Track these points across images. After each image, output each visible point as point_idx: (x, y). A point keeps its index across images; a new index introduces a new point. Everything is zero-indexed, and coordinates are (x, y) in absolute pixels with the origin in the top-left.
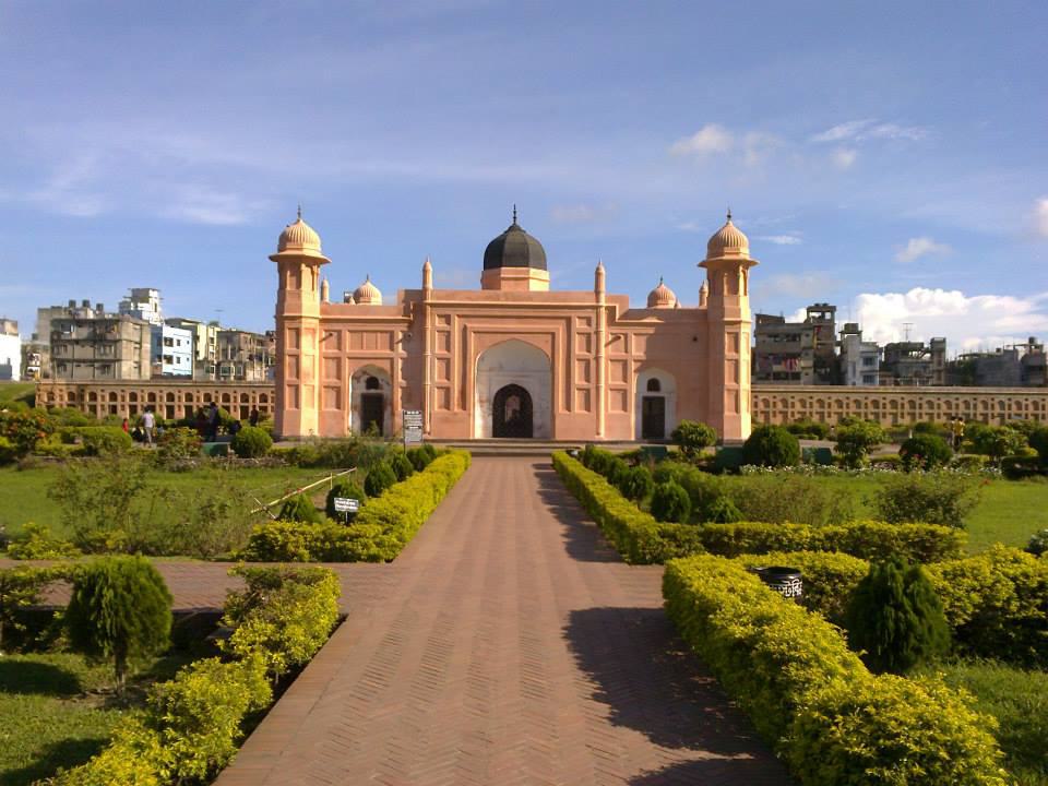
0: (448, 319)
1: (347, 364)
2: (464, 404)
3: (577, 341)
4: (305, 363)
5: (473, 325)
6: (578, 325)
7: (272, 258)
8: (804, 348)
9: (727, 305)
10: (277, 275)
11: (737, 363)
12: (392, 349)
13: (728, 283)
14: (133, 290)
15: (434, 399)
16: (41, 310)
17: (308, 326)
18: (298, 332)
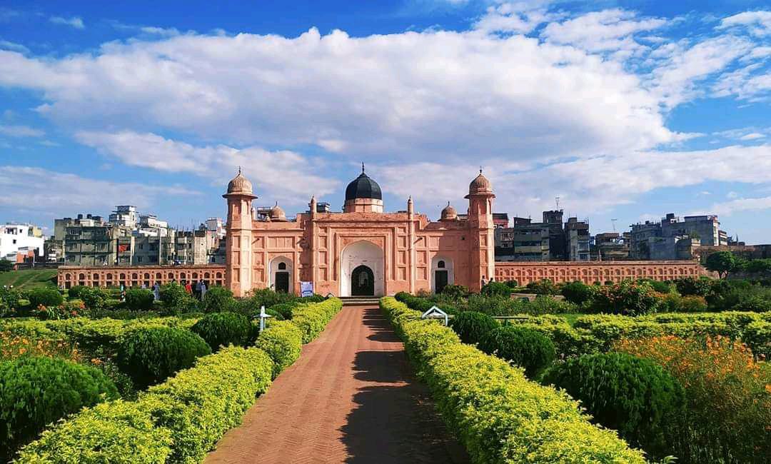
1: (267, 256)
2: (335, 278)
3: (399, 241)
5: (340, 232)
6: (399, 231)
7: (224, 196)
8: (543, 238)
9: (480, 218)
11: (486, 251)
12: (294, 247)
13: (480, 207)
14: (118, 207)
15: (318, 275)
16: (57, 221)
17: (246, 234)
18: (239, 237)
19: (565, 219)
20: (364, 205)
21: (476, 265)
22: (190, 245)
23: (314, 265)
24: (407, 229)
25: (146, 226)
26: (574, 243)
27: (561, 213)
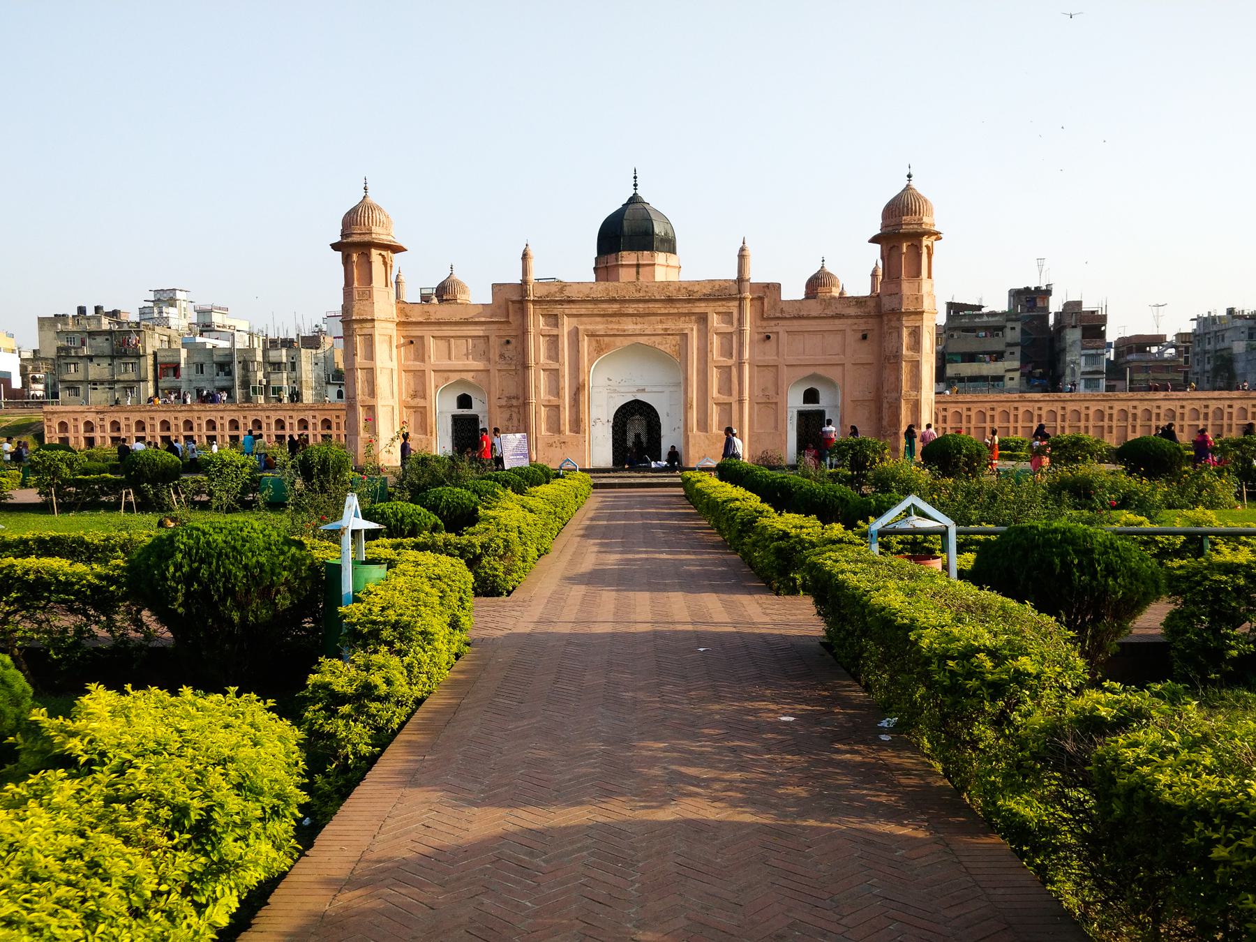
0: (554, 320)
1: (432, 379)
2: (577, 425)
3: (716, 341)
4: (382, 381)
5: (585, 325)
6: (715, 321)
8: (1009, 345)
9: (907, 288)
10: (342, 268)
11: (916, 366)
15: (539, 417)
19: (1055, 305)
20: (638, 266)
21: (894, 395)
22: (293, 364)
23: (533, 400)
24: (736, 315)
25: (206, 328)
26: (1076, 359)
27: (1048, 292)
